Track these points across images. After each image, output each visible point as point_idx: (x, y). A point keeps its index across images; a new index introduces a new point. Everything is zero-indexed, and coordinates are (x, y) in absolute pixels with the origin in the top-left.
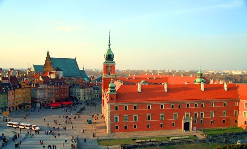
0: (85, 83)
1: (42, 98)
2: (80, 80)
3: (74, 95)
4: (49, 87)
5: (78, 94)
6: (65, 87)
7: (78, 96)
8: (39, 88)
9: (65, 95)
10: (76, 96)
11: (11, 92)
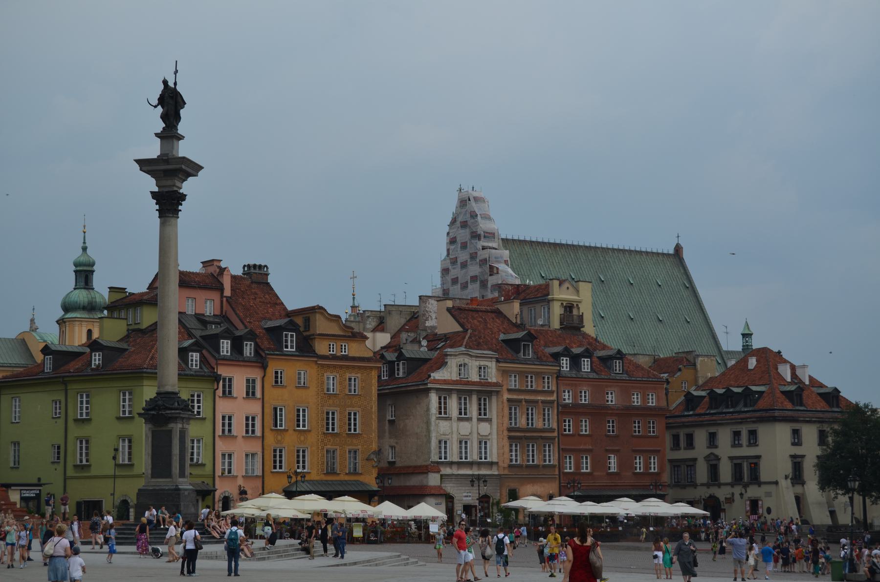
0: (789, 384)
1: (460, 464)
2: (752, 363)
3: (708, 485)
4: (513, 382)
5: (737, 469)
6: (636, 400)
7: (737, 490)
8: (436, 375)
9: (639, 465)
10: (722, 493)
11: (239, 377)
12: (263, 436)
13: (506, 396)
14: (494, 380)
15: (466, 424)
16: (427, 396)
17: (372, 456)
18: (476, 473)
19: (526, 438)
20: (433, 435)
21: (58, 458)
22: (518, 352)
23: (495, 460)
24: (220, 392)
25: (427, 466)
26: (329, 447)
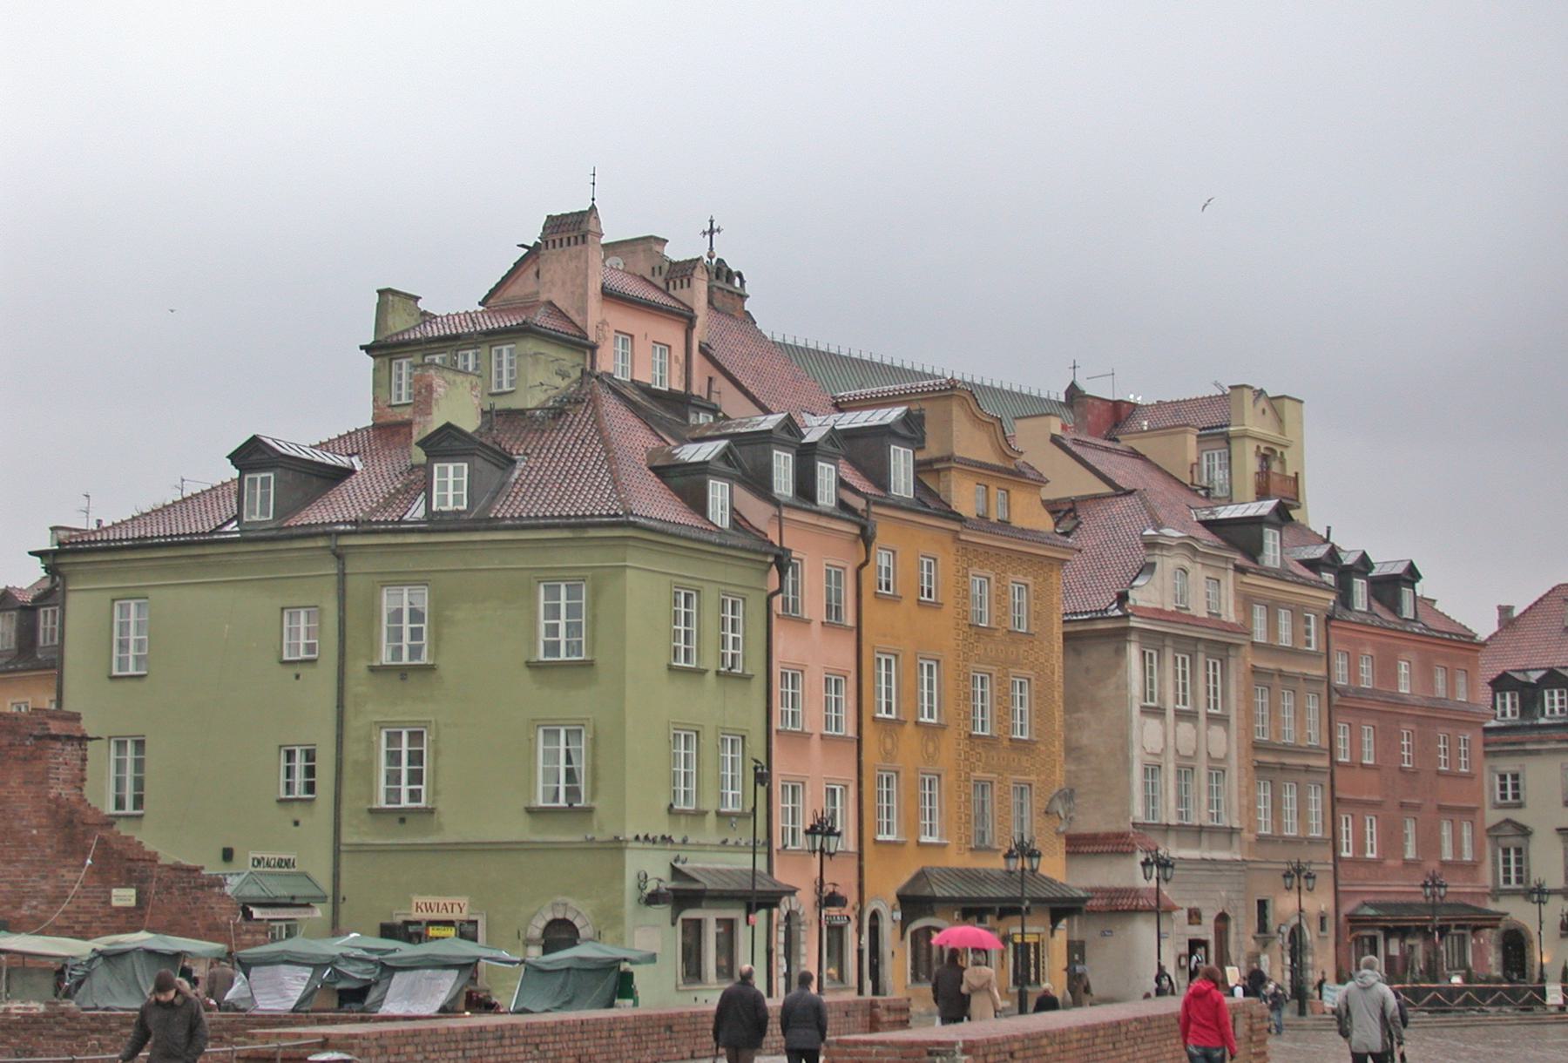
12: (859, 741)
13: (1250, 660)
14: (1230, 615)
15: (1185, 728)
16: (1120, 652)
17: (1059, 807)
18: (1207, 855)
19: (1283, 768)
20: (1136, 752)
21: (310, 788)
22: (1254, 550)
23: (1236, 825)
24: (777, 602)
25: (1120, 837)
26: (978, 774)
